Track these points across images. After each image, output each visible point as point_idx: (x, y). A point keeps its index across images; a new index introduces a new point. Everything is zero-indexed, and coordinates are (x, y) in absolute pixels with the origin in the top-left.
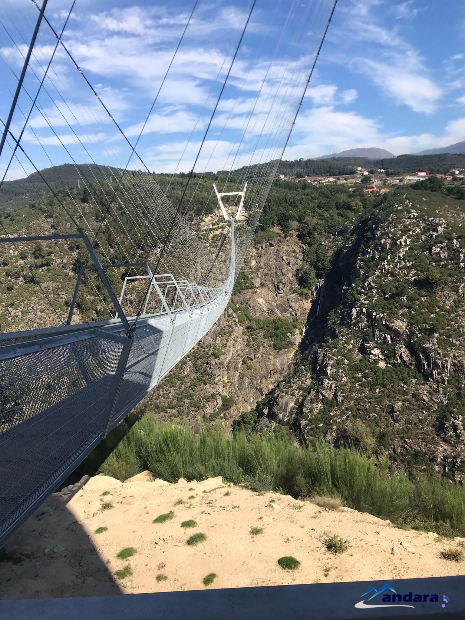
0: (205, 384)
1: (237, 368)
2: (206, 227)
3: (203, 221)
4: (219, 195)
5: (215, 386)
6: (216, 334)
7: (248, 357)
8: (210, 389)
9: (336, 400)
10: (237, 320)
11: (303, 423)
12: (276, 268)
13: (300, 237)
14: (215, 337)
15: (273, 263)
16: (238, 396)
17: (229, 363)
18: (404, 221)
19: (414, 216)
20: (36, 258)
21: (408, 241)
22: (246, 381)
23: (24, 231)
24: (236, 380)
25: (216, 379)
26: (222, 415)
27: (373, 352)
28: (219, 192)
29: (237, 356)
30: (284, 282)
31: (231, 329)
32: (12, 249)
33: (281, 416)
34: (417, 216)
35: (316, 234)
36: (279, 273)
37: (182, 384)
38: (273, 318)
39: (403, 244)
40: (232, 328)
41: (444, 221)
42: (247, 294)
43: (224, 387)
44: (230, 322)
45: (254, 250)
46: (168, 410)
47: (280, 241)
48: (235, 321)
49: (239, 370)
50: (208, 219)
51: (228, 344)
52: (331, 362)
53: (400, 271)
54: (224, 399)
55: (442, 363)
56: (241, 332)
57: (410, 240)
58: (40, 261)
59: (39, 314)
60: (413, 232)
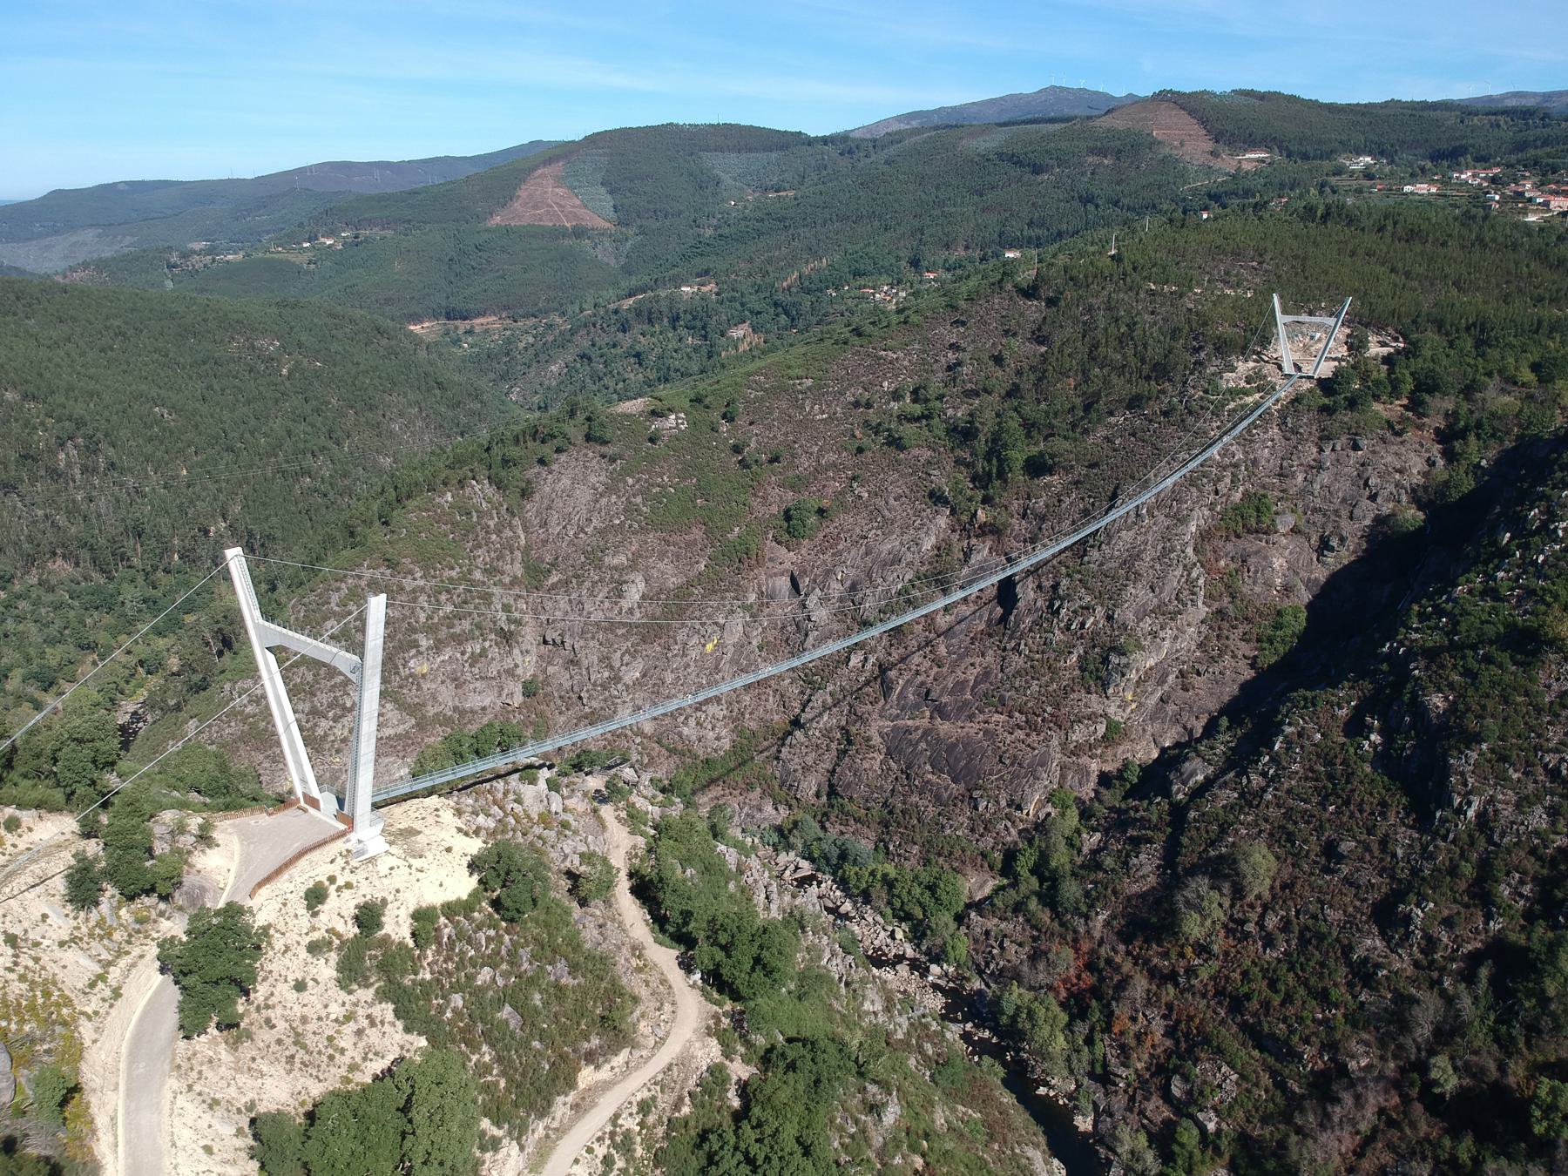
0: (1089, 693)
1: (1164, 682)
2: (1232, 384)
3: (1233, 369)
4: (1281, 319)
5: (1107, 702)
6: (1145, 611)
8: (1095, 703)
9: (1261, 797)
11: (1192, 814)
12: (1344, 500)
13: (1444, 437)
14: (1141, 616)
15: (1343, 488)
16: (1144, 730)
17: (1151, 668)
20: (915, 401)
22: (1171, 708)
23: (917, 346)
24: (1153, 701)
25: (1110, 691)
26: (1099, 752)
27: (1373, 737)
28: (1285, 312)
30: (1344, 533)
32: (886, 379)
33: (1175, 788)
35: (1472, 438)
36: (1344, 513)
37: (1052, 680)
38: (1287, 603)
40: (1185, 605)
42: (1251, 544)
43: (1119, 707)
44: (1186, 593)
45: (1315, 450)
46: (1017, 714)
47: (1384, 440)
49: (1166, 687)
50: (1244, 367)
51: (1162, 634)
52: (1288, 730)
54: (1112, 727)
55: (1461, 803)
58: (917, 409)
59: (892, 501)
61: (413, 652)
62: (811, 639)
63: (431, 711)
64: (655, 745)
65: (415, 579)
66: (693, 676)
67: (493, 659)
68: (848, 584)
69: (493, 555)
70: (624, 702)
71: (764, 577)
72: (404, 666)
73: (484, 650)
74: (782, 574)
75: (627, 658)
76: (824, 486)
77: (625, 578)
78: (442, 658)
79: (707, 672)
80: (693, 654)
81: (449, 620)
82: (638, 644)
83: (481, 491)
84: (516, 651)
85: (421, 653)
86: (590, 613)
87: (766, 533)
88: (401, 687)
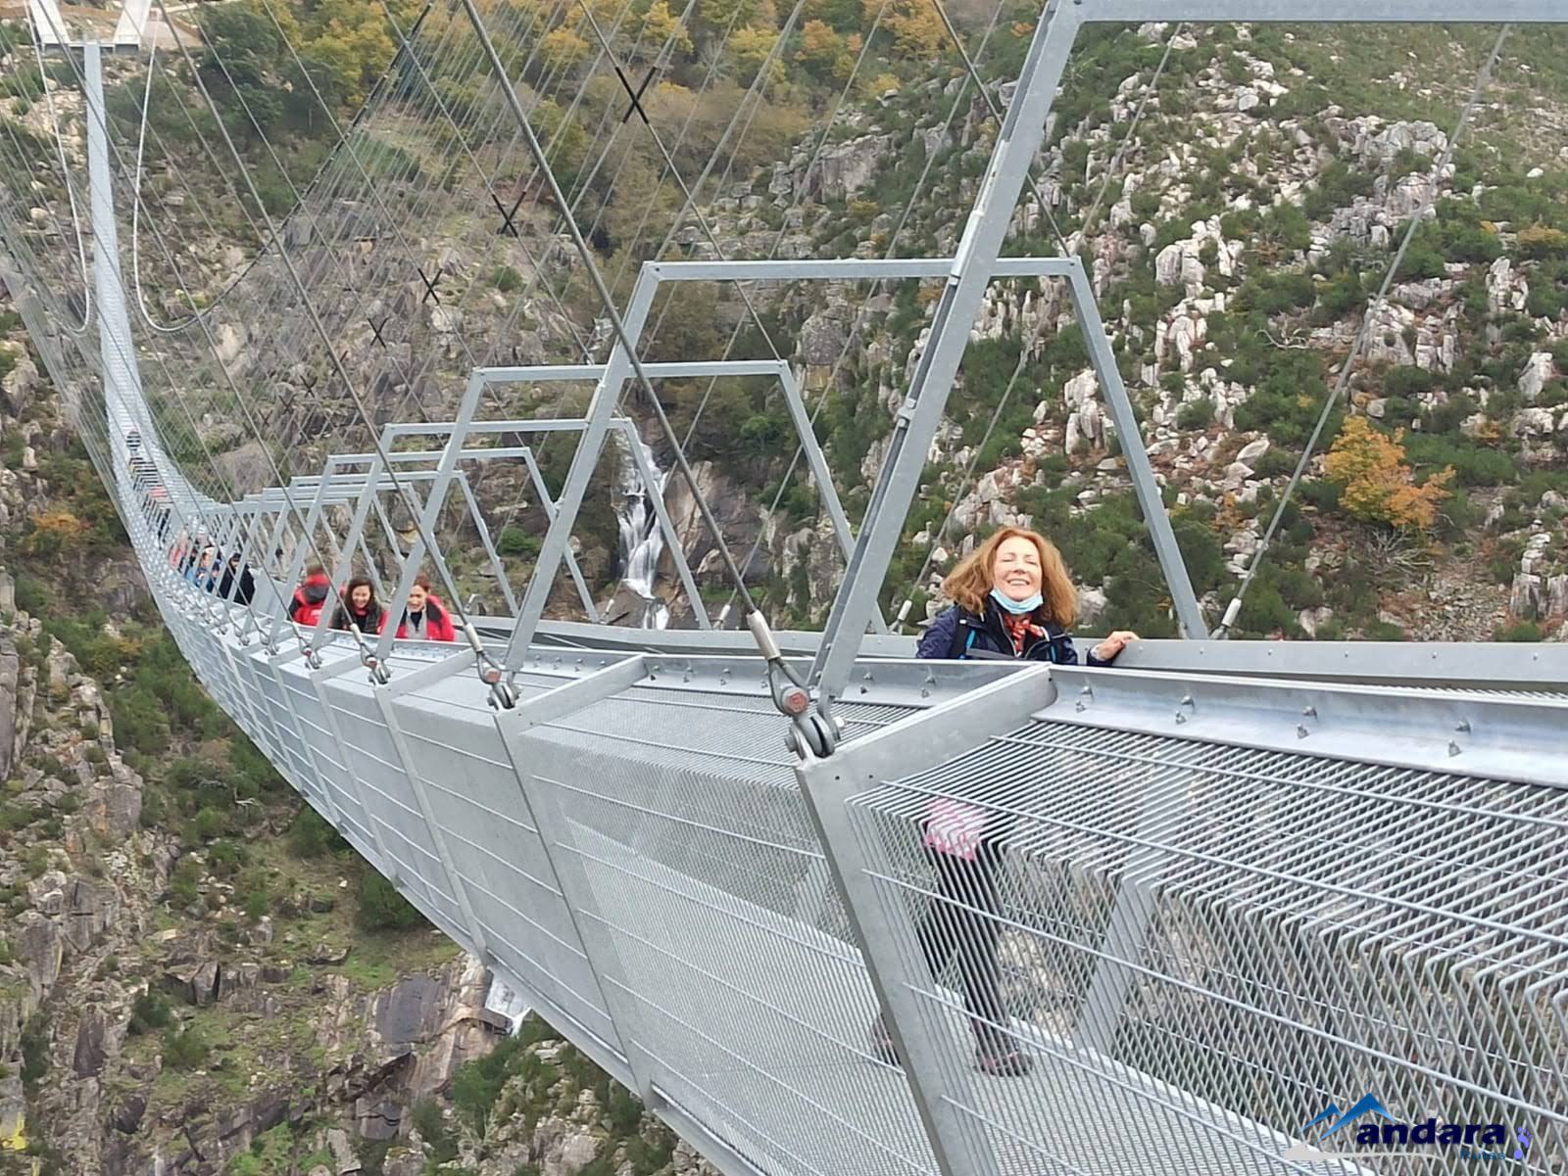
7: (172, 979)
10: (106, 729)
18: (1201, 124)
19: (1265, 97)
21: (1223, 255)
29: (99, 977)
31: (56, 788)
34: (1280, 97)
39: (1195, 269)
41: (1440, 139)
45: (236, 254)
48: (90, 734)
53: (1175, 442)
56: (133, 810)
57: (1236, 247)
60: (1261, 196)
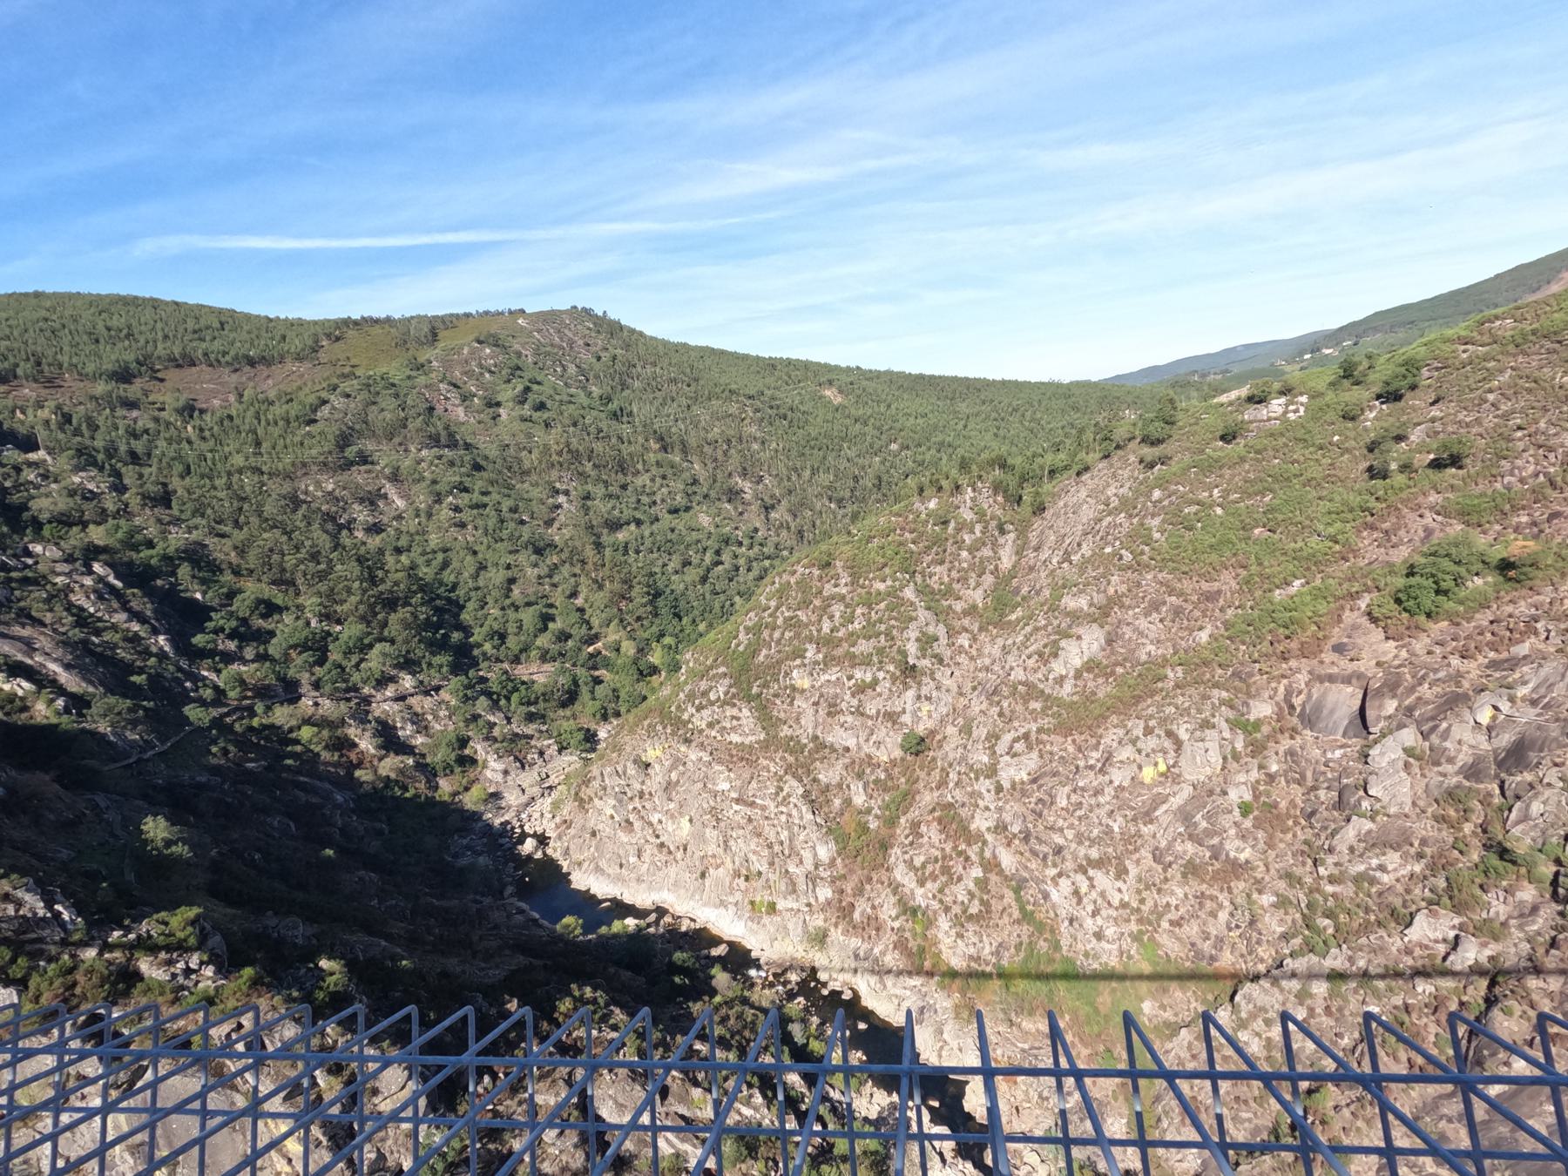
61: (798, 662)
62: (1350, 833)
63: (785, 731)
64: (1009, 897)
65: (836, 586)
66: (1103, 812)
67: (880, 695)
68: (1506, 739)
69: (954, 574)
70: (987, 808)
71: (1302, 679)
72: (787, 674)
73: (875, 682)
74: (1347, 680)
75: (1020, 747)
76: (1555, 515)
77: (1074, 630)
78: (827, 677)
79: (1130, 814)
80: (1119, 776)
81: (852, 638)
82: (1048, 732)
83: (973, 501)
84: (910, 694)
85: (805, 666)
86: (1012, 669)
87: (1354, 596)
88: (776, 695)
